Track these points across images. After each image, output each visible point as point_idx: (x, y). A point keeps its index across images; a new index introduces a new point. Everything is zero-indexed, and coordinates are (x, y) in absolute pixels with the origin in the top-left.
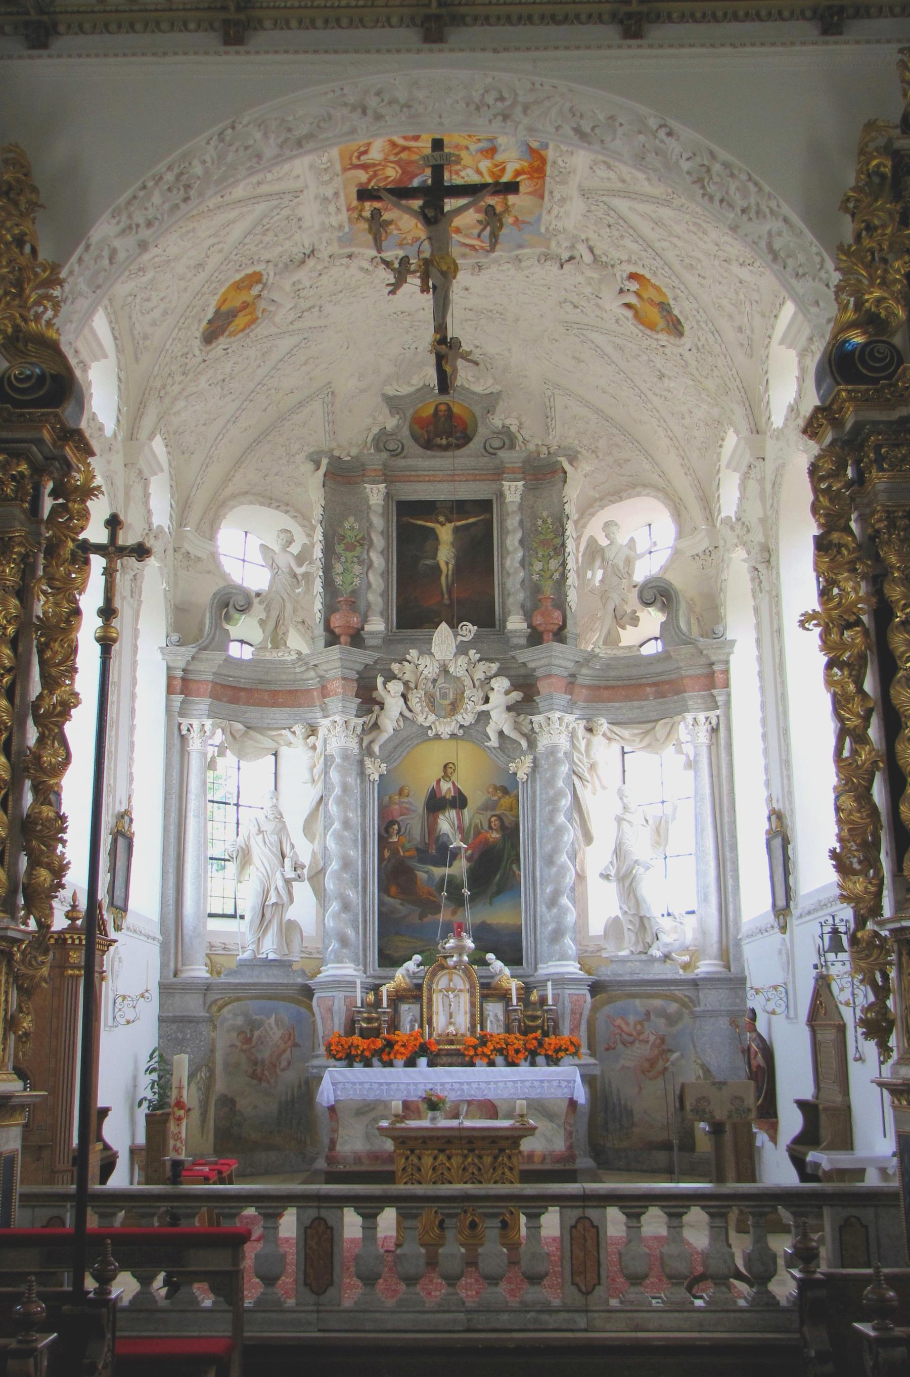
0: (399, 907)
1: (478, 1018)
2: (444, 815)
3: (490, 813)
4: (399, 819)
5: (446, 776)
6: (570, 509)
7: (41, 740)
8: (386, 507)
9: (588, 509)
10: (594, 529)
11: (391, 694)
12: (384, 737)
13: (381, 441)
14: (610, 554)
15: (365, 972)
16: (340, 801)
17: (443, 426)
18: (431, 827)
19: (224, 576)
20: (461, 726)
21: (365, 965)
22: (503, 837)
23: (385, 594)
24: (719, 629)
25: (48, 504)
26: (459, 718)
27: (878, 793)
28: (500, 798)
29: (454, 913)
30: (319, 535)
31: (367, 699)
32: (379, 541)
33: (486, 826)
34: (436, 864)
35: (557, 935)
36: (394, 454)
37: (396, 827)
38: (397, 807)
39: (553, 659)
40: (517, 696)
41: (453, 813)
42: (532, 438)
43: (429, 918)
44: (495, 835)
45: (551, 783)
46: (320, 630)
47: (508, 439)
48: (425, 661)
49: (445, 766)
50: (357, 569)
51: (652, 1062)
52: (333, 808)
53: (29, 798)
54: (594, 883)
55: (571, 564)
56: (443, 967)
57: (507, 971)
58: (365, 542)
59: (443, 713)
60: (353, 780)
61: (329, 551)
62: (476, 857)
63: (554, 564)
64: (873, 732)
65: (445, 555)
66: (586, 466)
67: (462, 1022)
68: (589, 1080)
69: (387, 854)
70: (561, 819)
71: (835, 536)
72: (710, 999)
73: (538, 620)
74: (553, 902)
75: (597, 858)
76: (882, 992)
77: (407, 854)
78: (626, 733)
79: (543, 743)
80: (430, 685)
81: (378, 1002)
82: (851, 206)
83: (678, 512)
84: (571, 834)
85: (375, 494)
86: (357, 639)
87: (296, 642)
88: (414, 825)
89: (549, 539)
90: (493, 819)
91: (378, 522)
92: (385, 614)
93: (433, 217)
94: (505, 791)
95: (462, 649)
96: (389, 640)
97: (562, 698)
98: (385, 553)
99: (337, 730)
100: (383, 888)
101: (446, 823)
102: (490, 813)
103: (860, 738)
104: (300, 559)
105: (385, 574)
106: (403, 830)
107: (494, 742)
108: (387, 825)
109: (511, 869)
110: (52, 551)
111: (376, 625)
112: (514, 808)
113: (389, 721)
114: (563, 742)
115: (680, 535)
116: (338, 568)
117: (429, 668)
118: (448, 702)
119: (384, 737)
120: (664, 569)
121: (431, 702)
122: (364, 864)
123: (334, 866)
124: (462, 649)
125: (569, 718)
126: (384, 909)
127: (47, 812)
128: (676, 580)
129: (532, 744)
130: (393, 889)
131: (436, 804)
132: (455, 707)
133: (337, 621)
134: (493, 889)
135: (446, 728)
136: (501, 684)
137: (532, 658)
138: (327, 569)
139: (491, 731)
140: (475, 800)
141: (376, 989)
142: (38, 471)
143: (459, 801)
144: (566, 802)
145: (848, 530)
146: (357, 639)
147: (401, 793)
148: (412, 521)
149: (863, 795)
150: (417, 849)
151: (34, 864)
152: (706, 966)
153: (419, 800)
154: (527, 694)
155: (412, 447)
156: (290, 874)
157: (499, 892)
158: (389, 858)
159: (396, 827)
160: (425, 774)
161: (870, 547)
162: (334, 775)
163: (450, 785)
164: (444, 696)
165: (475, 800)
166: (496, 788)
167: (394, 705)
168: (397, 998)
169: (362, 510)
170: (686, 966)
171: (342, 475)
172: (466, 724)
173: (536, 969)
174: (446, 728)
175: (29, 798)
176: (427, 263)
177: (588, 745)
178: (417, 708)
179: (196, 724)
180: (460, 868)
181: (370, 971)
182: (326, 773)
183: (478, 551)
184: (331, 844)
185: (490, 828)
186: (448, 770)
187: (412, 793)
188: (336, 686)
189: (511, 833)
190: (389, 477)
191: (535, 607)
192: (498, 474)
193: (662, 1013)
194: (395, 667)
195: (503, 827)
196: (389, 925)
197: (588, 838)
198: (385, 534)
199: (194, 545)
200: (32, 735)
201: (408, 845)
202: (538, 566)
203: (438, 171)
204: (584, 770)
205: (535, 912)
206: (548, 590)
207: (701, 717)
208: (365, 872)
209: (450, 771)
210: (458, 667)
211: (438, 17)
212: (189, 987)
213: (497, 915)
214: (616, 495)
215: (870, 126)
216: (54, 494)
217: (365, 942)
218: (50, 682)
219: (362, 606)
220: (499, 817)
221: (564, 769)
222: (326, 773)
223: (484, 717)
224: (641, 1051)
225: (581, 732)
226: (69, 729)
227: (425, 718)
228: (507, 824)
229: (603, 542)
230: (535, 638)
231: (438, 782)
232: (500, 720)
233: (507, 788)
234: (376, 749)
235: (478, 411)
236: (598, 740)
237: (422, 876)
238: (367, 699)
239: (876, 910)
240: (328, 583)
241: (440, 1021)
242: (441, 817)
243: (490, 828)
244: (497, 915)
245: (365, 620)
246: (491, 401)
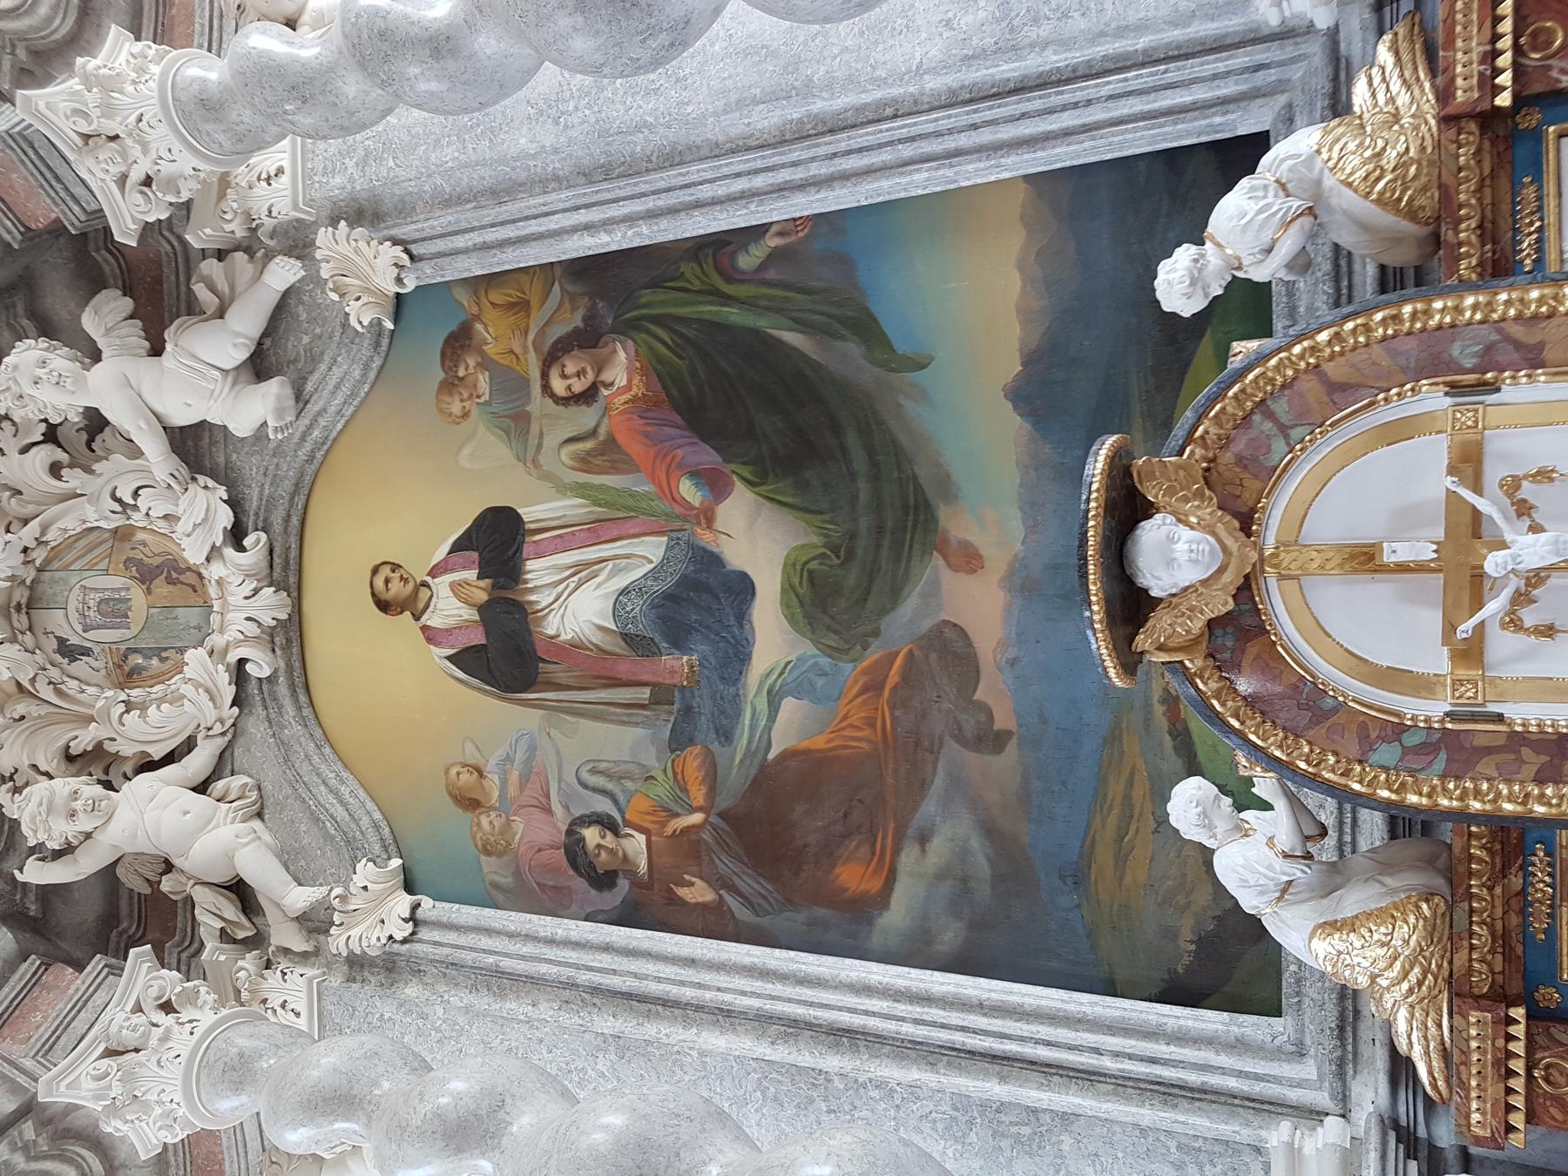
0: (939, 848)
2: (540, 616)
3: (538, 404)
4: (562, 820)
15: (1315, 1115)
18: (593, 668)
20: (236, 535)
21: (1269, 1108)
22: (626, 328)
26: (194, 554)
28: (485, 364)
29: (970, 560)
33: (585, 417)
34: (738, 654)
37: (591, 835)
38: (519, 826)
41: (539, 571)
43: (996, 693)
44: (621, 369)
49: (384, 606)
56: (1240, 628)
59: (189, 616)
62: (707, 456)
69: (697, 892)
77: (698, 795)
80: (80, 667)
88: (592, 750)
90: (558, 386)
94: (459, 342)
100: (844, 927)
101: (577, 603)
102: (538, 404)
106: (604, 806)
108: (585, 878)
109: (756, 277)
118: (137, 595)
119: (258, 865)
122: (725, 1016)
126: (950, 936)
130: (852, 876)
131: (506, 654)
132: (168, 574)
134: (846, 358)
140: (485, 473)
143: (497, 542)
147: (470, 803)
150: (679, 741)
153: (496, 723)
157: (866, 328)
158: (721, 883)
159: (591, 835)
163: (442, 584)
164: (114, 611)
165: (485, 473)
166: (450, 385)
167: (155, 817)
172: (225, 517)
173: (1287, 34)
174: (241, 602)
180: (756, 538)
181: (1304, 1078)
185: (588, 396)
186: (396, 600)
187: (471, 755)
189: (610, 289)
195: (587, 339)
201: (661, 790)
205: (953, 100)
208: (762, 1022)
209: (397, 589)
213: (971, 325)
217: (1123, 1085)
220: (551, 359)
223: (194, 447)
227: (194, 696)
228: (577, 320)
231: (430, 635)
232: (197, 376)
233: (441, 328)
242: (551, 626)
243: (588, 396)
244: (971, 325)
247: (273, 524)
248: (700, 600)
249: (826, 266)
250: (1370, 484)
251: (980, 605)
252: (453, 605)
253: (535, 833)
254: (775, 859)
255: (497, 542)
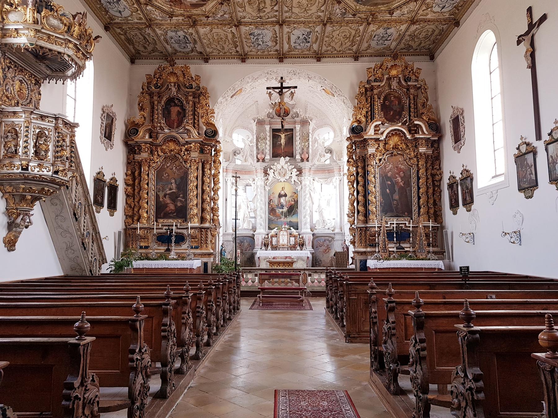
1: (289, 241)
5: (283, 190)
6: (310, 131)
7: (214, 194)
8: (270, 130)
9: (314, 130)
10: (315, 135)
11: (271, 172)
12: (269, 181)
13: (269, 115)
14: (319, 141)
16: (260, 195)
17: (282, 112)
18: (279, 201)
19: (234, 145)
23: (270, 150)
24: (342, 159)
25: (213, 153)
27: (355, 204)
30: (255, 137)
31: (266, 173)
32: (268, 138)
35: (305, 224)
36: (272, 118)
39: (306, 165)
40: (298, 173)
42: (302, 115)
44: (293, 203)
45: (305, 192)
46: (255, 158)
47: (297, 115)
48: (278, 165)
50: (263, 145)
51: (326, 250)
52: (258, 197)
53: (212, 204)
54: (314, 213)
55: (310, 143)
57: (295, 231)
58: (265, 138)
60: (263, 191)
61: (257, 141)
63: (306, 144)
64: (355, 194)
65: (283, 141)
66: (314, 121)
67: (285, 242)
68: (312, 254)
70: (307, 199)
71: (350, 160)
72: (337, 237)
73: (303, 156)
74: (305, 217)
75: (315, 207)
76: (354, 237)
78: (322, 180)
79: (303, 183)
81: (268, 238)
82: (357, 97)
83: (335, 131)
84: (309, 203)
85: (267, 127)
86: (263, 160)
87: (250, 161)
89: (306, 138)
91: (268, 134)
92: (270, 155)
93: (281, 94)
95: (286, 163)
96: (270, 160)
97: (307, 174)
98: (270, 141)
99: (260, 178)
100: (269, 214)
101: (282, 200)
103: (353, 195)
104: (251, 142)
105: (270, 146)
107: (293, 183)
108: (270, 200)
110: (214, 162)
111: (268, 157)
112: (297, 197)
113: (271, 177)
114: (308, 183)
115: (335, 137)
116: (259, 144)
117: (279, 167)
119: (269, 181)
120: (331, 144)
121: (279, 174)
123: (259, 209)
124: (286, 163)
125: (309, 178)
127: (216, 207)
128: (333, 148)
129: (301, 183)
131: (280, 196)
133: (259, 157)
135: (282, 180)
136: (295, 170)
137: (301, 165)
138: (257, 144)
139: (292, 180)
141: (268, 234)
142: (212, 147)
143: (285, 195)
144: (308, 196)
145: (353, 158)
146: (263, 160)
148: (275, 133)
149: (352, 205)
151: (214, 215)
152: (337, 231)
153: (277, 195)
154: (300, 171)
155: (276, 117)
156: (249, 211)
160: (278, 190)
161: (356, 162)
162: (259, 190)
167: (271, 175)
168: (272, 237)
169: (264, 131)
170: (333, 231)
171: (260, 123)
174: (282, 180)
175: (212, 204)
176: (280, 103)
177: (313, 183)
178: (276, 175)
179: (229, 179)
180: (285, 209)
182: (257, 189)
183: (290, 140)
184: (258, 204)
188: (259, 171)
189: (296, 202)
190: (270, 124)
191: (303, 153)
192: (295, 123)
193: (328, 240)
194: (272, 166)
196: (270, 221)
197: (313, 203)
198: (270, 136)
199: (228, 139)
200: (213, 193)
202: (303, 144)
203: (282, 84)
204: (312, 189)
206: (305, 149)
207: (338, 178)
210: (286, 167)
211: (282, 58)
212: (228, 234)
213: (293, 219)
214: (321, 127)
215: (361, 82)
216: (214, 151)
218: (215, 184)
219: (265, 153)
221: (308, 189)
222: (257, 189)
223: (291, 177)
224: (323, 248)
225: (312, 180)
226: (219, 193)
227: (278, 177)
229: (318, 138)
230: (302, 160)
232: (294, 178)
234: (268, 184)
235: (290, 108)
236: (315, 182)
237: (277, 211)
238: (266, 173)
239: (354, 223)
240: (257, 148)
241: (281, 242)
245: (265, 156)
246: (294, 106)
247: (287, 181)
248: (282, 206)
249: (296, 213)
250: (285, 233)
251: (282, 219)
252: (283, 193)
253: (272, 198)
254: (272, 211)
255: (285, 195)
